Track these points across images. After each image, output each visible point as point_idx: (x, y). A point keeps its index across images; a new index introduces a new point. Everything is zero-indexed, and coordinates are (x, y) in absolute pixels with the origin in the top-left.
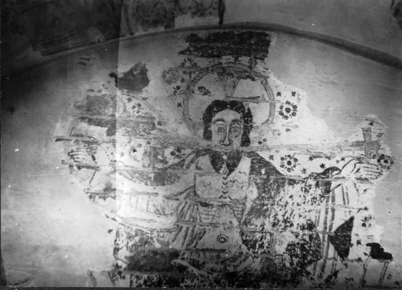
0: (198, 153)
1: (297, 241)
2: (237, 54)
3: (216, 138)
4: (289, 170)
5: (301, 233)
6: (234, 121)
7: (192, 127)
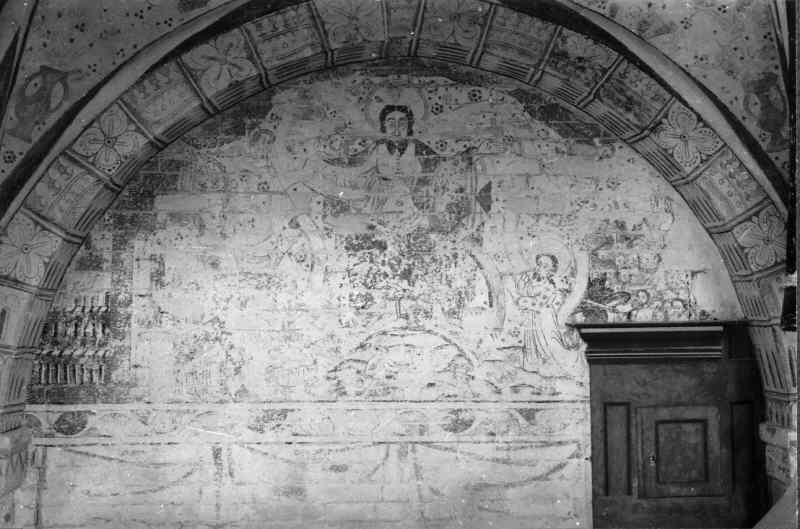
0: (378, 143)
1: (453, 201)
2: (399, 73)
3: (389, 131)
4: (442, 150)
5: (455, 195)
6: (401, 119)
7: (373, 124)
